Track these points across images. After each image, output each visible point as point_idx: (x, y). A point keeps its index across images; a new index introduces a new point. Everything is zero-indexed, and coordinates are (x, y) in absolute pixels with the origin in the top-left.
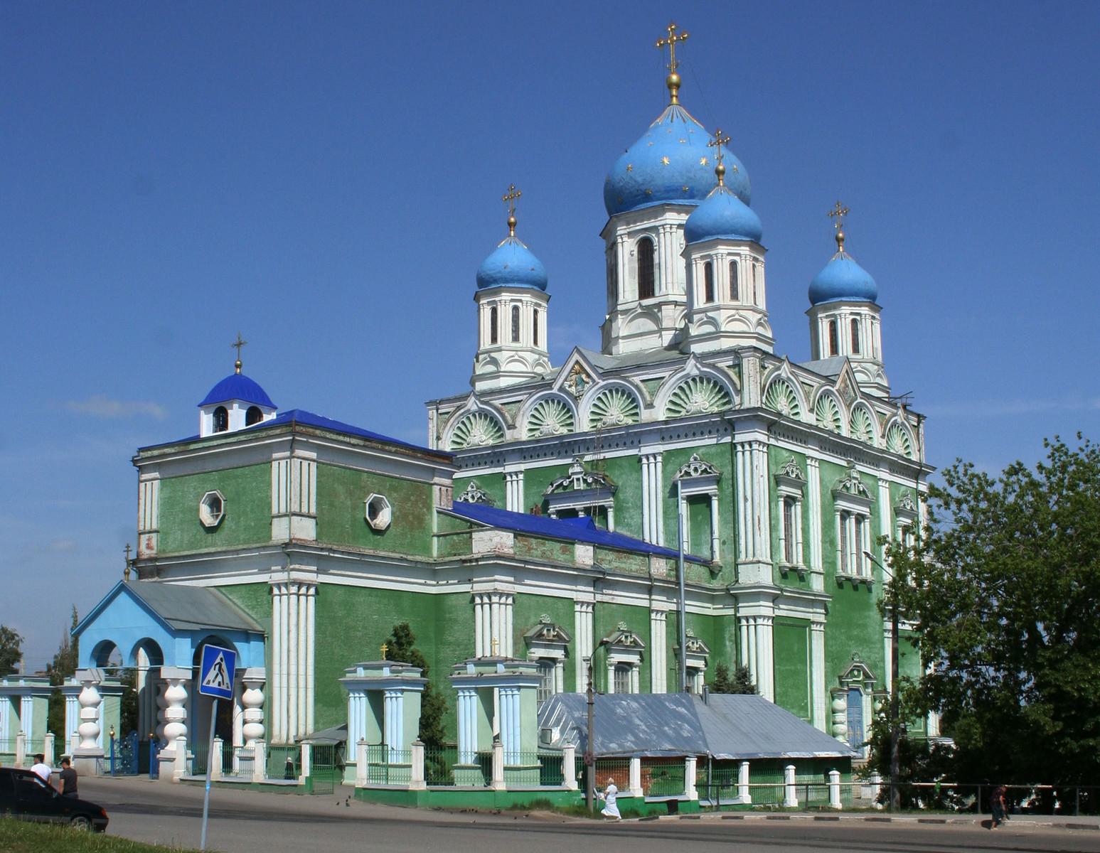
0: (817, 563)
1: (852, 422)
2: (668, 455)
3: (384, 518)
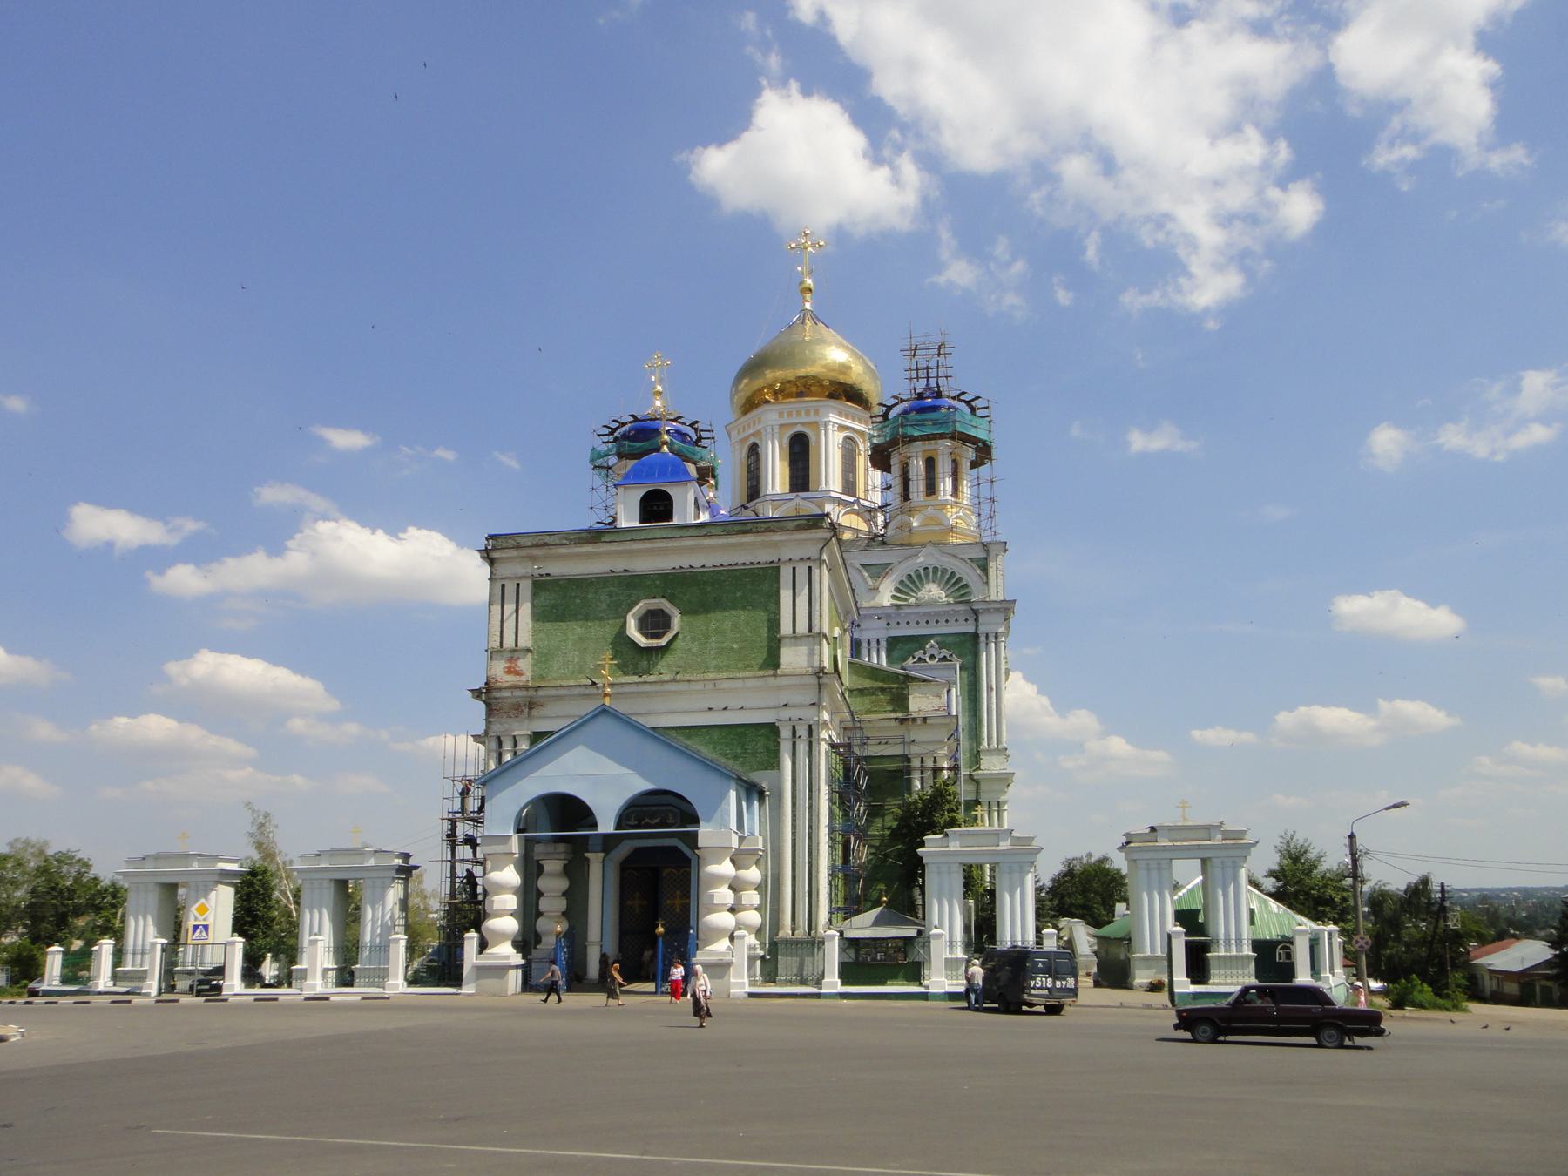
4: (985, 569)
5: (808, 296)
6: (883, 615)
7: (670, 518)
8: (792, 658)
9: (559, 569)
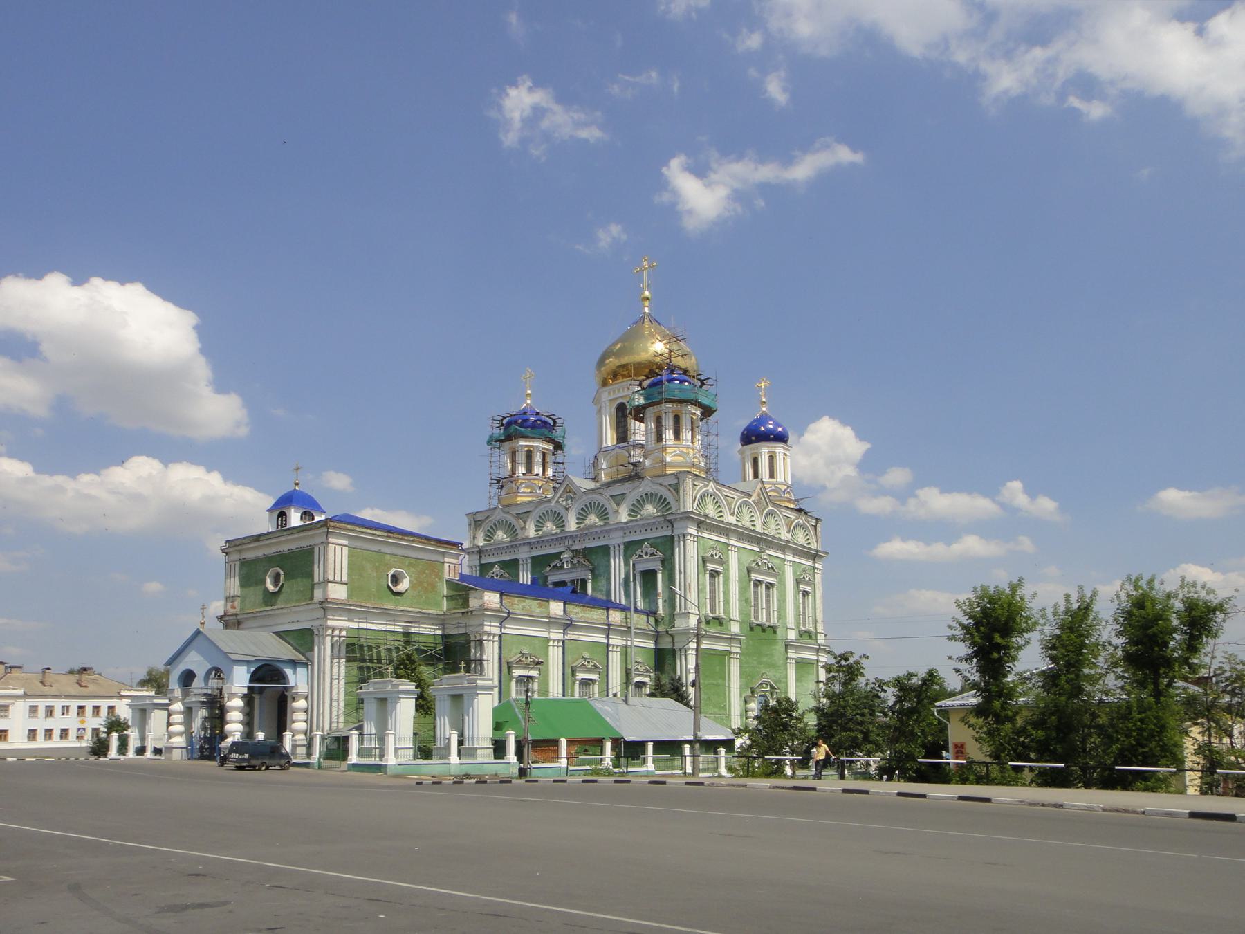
0: (735, 614)
1: (765, 523)
3: (403, 586)
4: (677, 491)
5: (647, 303)
6: (625, 527)
8: (318, 594)
9: (249, 555)
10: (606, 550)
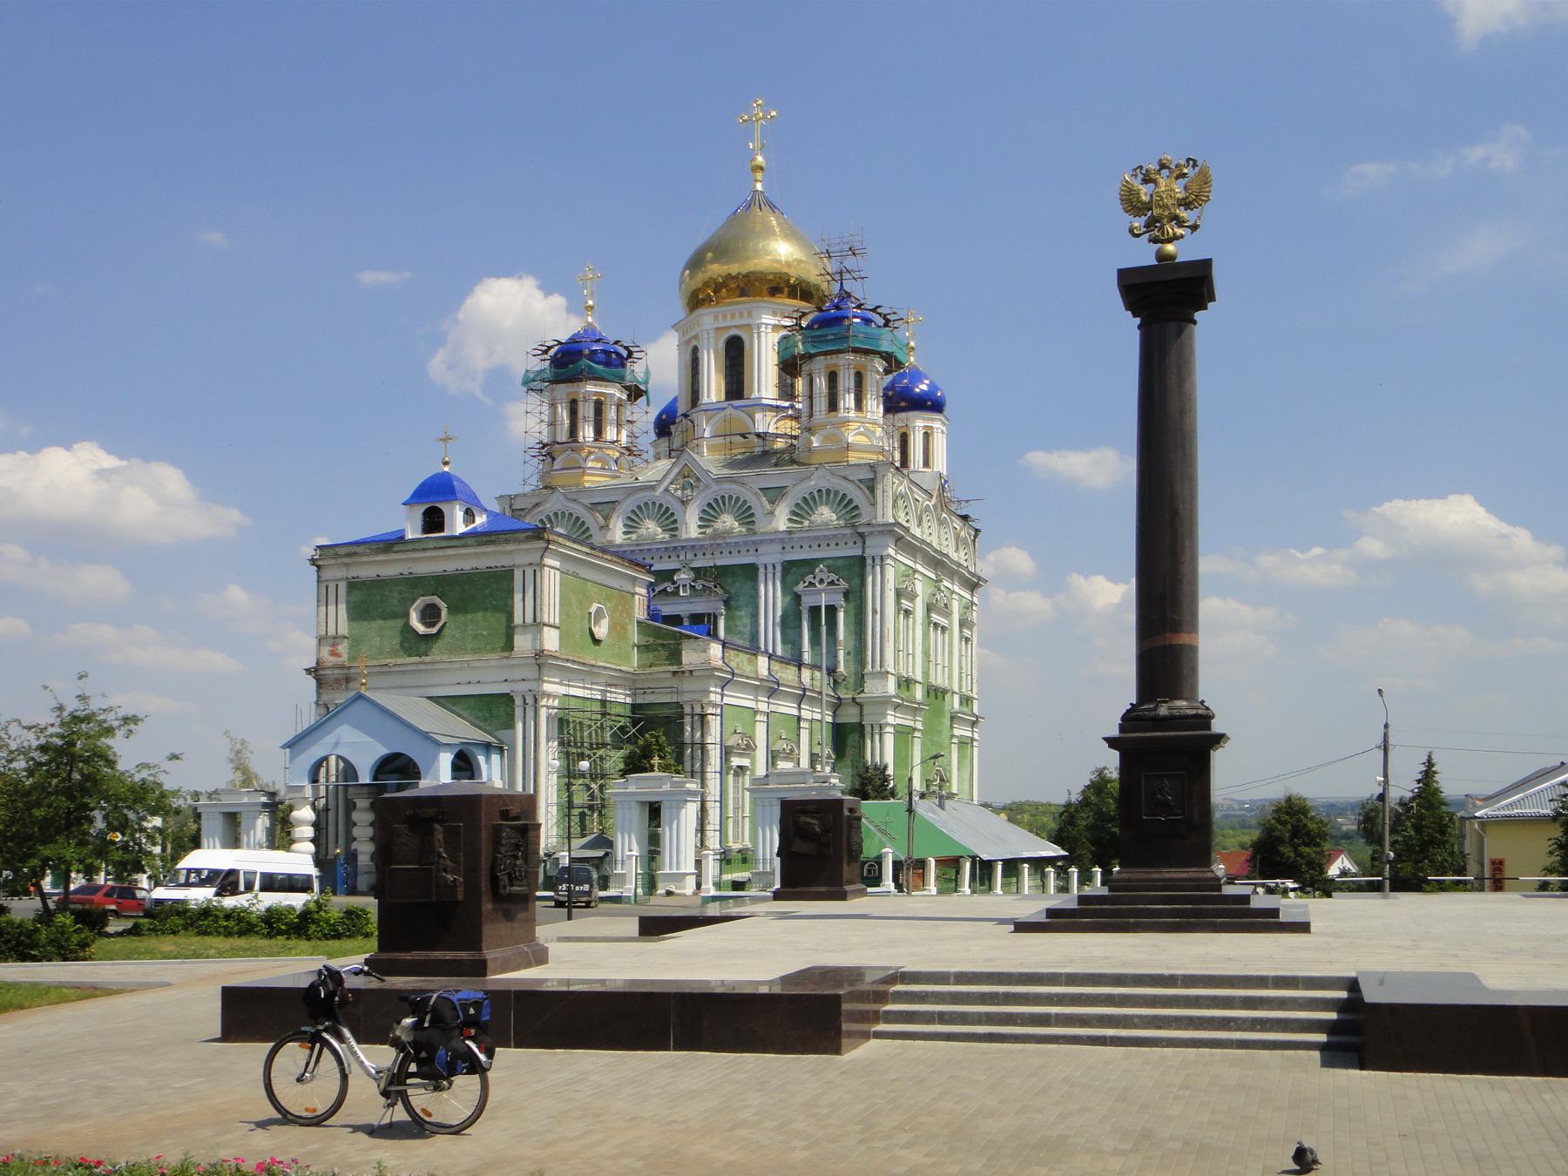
2: (788, 567)
4: (872, 490)
7: (441, 529)
8: (522, 642)
10: (750, 572)
